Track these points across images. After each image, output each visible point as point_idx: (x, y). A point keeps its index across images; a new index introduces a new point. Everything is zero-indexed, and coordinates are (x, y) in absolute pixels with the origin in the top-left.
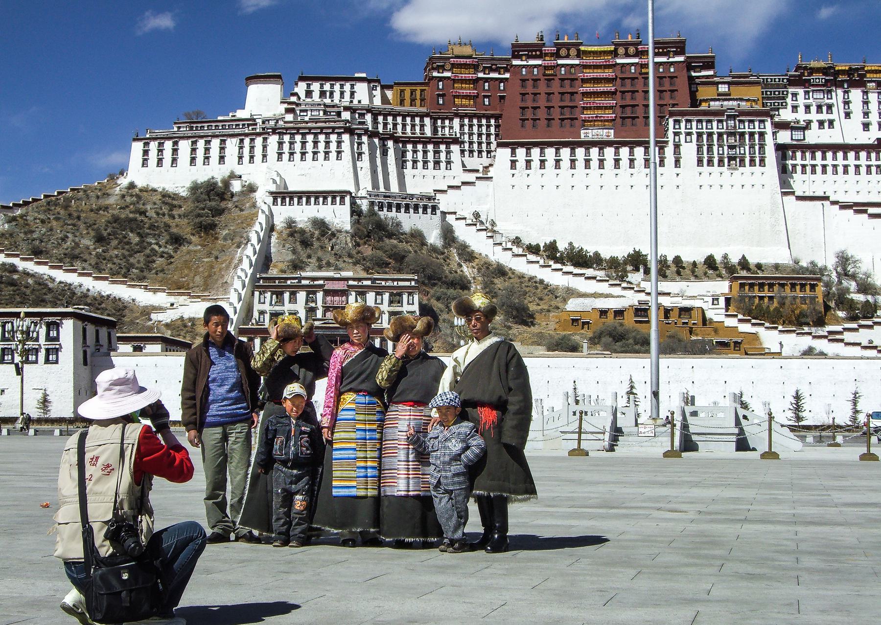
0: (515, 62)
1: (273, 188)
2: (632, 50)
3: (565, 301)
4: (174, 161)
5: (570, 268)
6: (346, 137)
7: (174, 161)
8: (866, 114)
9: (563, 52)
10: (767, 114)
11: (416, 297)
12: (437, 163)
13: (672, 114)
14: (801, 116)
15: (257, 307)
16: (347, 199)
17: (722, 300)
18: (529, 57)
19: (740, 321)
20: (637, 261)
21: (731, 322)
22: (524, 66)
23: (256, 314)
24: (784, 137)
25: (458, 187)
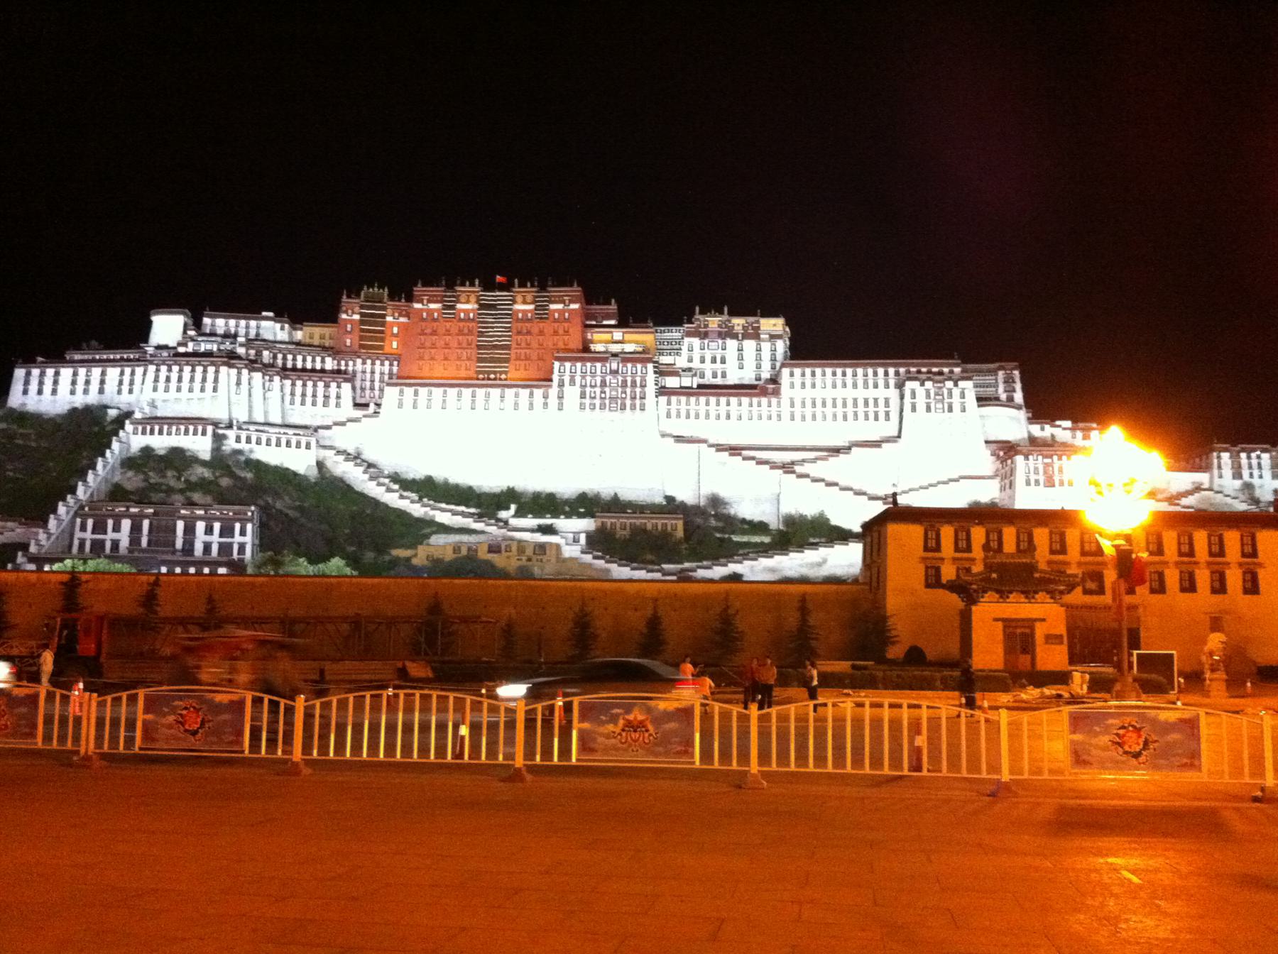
0: (417, 306)
1: (138, 415)
2: (529, 297)
3: (428, 536)
4: (54, 392)
5: (443, 505)
6: (223, 369)
7: (54, 392)
8: (759, 367)
9: (463, 298)
10: (650, 360)
11: (249, 526)
12: (326, 397)
13: (558, 359)
14: (696, 364)
15: (78, 534)
16: (210, 429)
17: (583, 538)
18: (429, 301)
19: (595, 558)
20: (508, 497)
21: (588, 558)
22: (422, 310)
23: (76, 542)
24: (672, 382)
25: (343, 424)
